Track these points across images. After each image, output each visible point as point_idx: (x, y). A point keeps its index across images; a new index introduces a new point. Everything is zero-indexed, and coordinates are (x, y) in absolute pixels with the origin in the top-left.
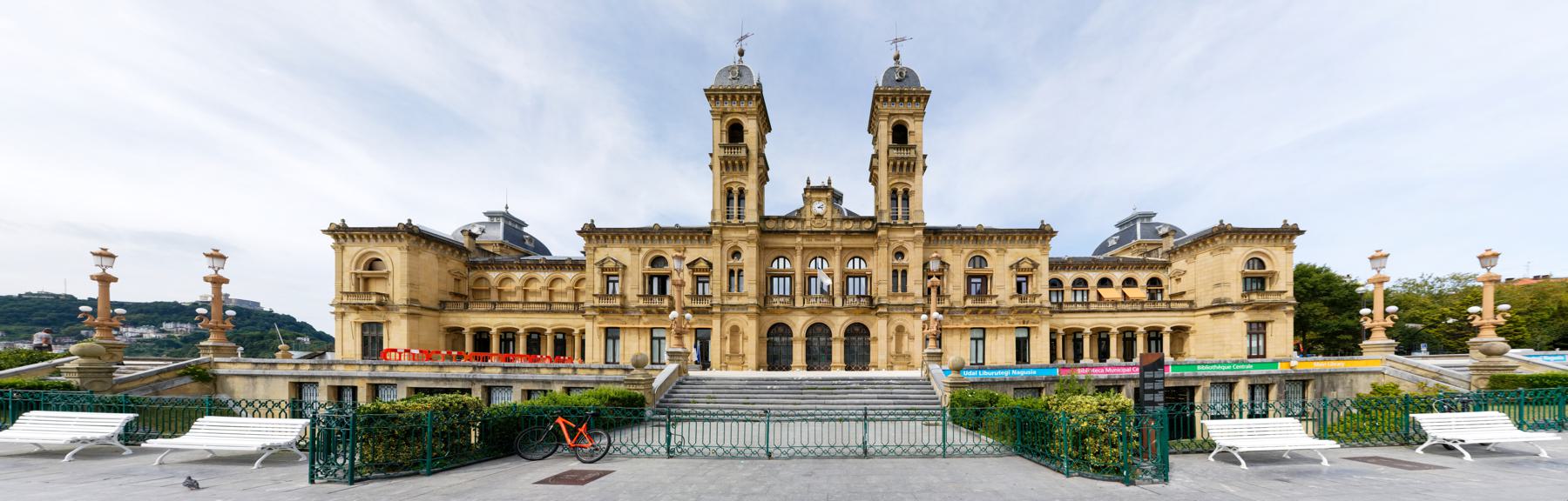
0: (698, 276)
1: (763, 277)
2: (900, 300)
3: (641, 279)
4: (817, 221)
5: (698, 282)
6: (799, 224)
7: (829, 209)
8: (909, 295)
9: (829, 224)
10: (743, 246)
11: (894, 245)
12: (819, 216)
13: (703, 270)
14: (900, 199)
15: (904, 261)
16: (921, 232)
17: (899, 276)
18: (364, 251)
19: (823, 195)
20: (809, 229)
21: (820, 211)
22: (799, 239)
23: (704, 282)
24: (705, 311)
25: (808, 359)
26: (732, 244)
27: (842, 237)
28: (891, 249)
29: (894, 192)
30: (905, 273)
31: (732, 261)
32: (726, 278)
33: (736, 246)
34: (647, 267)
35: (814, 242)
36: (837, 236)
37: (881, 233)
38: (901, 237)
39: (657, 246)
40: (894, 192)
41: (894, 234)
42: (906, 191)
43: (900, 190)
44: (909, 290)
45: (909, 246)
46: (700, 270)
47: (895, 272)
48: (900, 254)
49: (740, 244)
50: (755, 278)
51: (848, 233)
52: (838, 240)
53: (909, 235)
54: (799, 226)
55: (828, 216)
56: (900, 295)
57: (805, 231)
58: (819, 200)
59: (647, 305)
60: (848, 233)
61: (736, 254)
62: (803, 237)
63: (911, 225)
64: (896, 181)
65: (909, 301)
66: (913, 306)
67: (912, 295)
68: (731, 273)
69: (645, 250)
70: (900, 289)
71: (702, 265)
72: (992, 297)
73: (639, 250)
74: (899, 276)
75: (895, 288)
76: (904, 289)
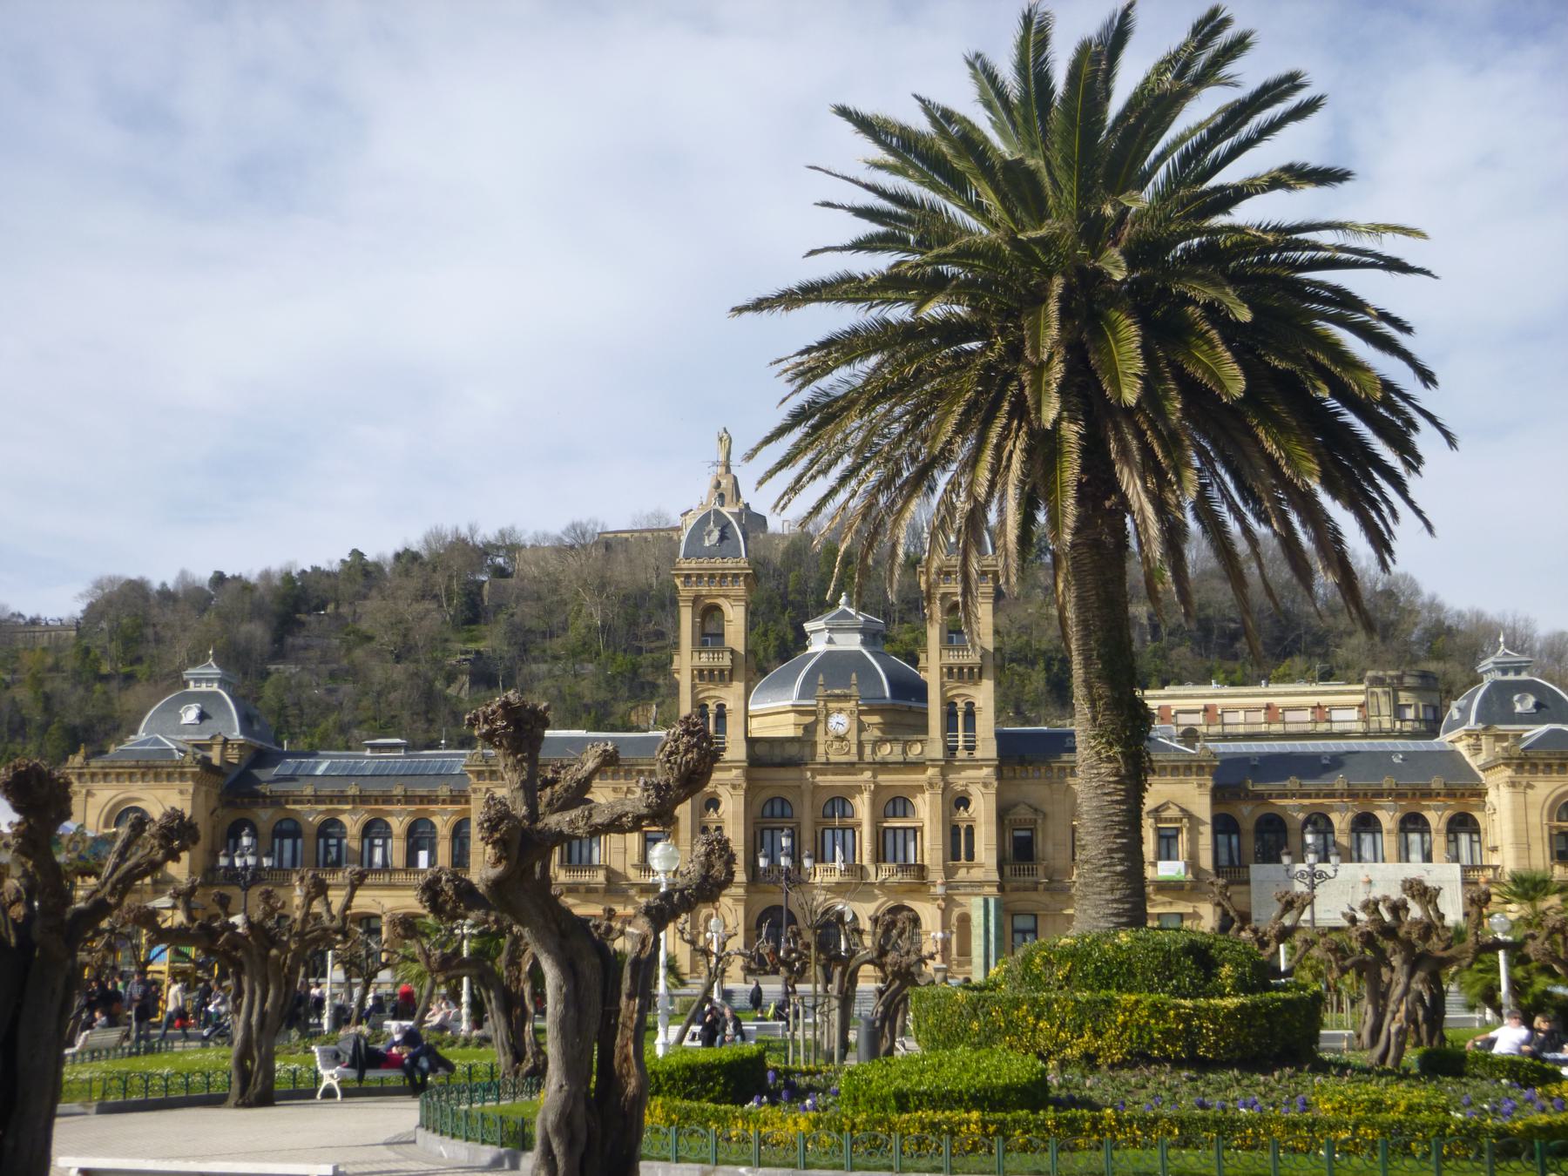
1: (751, 832)
4: (836, 745)
9: (854, 749)
18: (121, 797)
21: (841, 730)
30: (970, 831)
51: (884, 766)
58: (840, 711)
60: (884, 766)
67: (980, 866)
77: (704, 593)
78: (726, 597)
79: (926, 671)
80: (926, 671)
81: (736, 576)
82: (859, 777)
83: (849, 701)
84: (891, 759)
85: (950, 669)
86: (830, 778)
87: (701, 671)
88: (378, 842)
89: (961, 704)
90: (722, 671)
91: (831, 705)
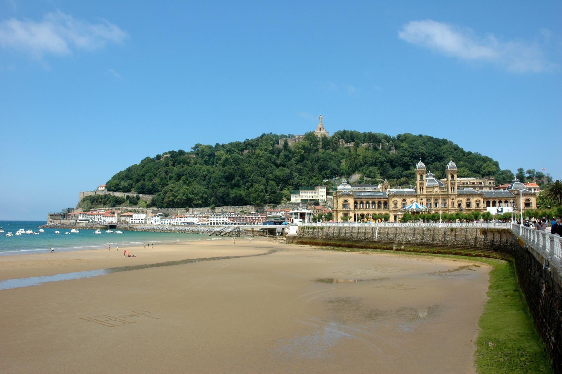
2: (453, 209)
10: (423, 198)
11: (451, 198)
12: (437, 192)
17: (453, 204)
19: (437, 187)
21: (437, 190)
22: (433, 196)
30: (454, 203)
39: (404, 197)
40: (452, 187)
47: (452, 203)
51: (442, 195)
52: (440, 196)
54: (433, 193)
65: (455, 209)
66: (455, 210)
72: (471, 207)
74: (453, 204)
76: (454, 206)
88: (367, 204)
89: (453, 188)
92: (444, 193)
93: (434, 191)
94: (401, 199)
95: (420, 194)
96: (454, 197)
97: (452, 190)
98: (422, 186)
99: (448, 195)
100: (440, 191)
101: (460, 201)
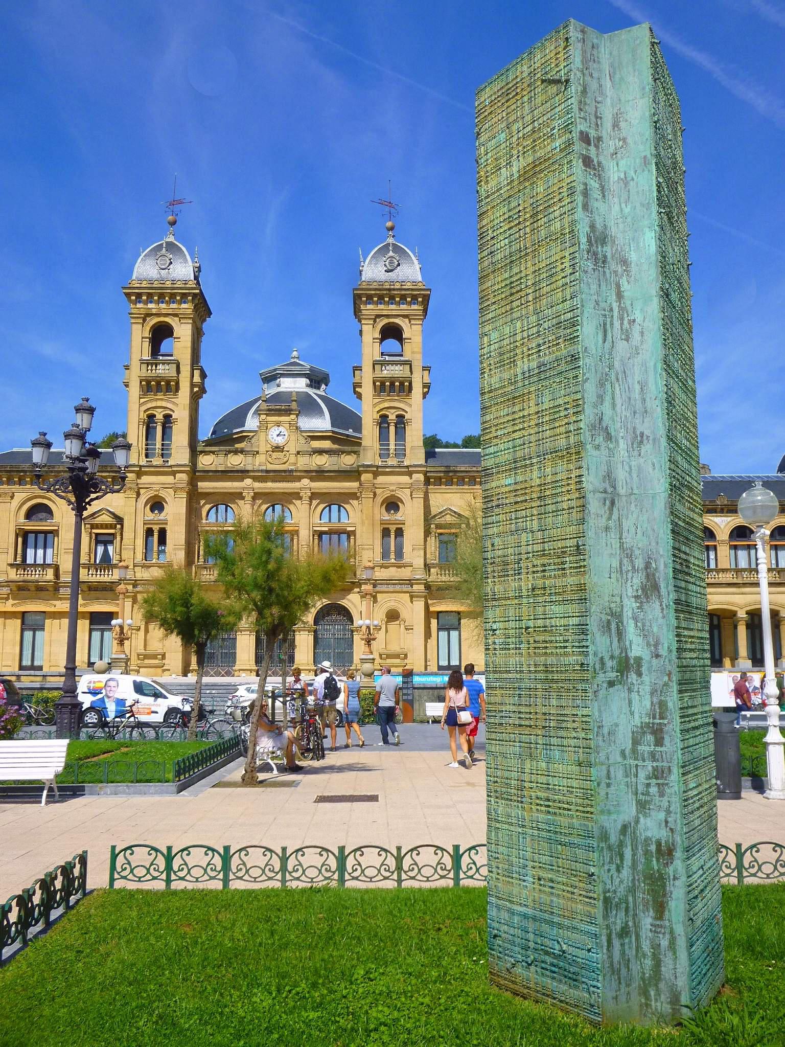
0: (97, 535)
2: (392, 573)
3: (13, 537)
4: (275, 455)
5: (98, 542)
6: (249, 459)
7: (293, 438)
8: (404, 566)
9: (292, 459)
10: (167, 495)
11: (382, 495)
12: (278, 449)
13: (107, 526)
14: (392, 429)
15: (399, 516)
16: (421, 477)
20: (264, 468)
21: (280, 441)
23: (106, 543)
24: (107, 590)
25: (258, 660)
26: (151, 493)
27: (312, 479)
28: (379, 500)
29: (384, 418)
30: (399, 533)
31: (150, 516)
32: (140, 542)
33: (156, 496)
34: (22, 519)
35: (270, 486)
36: (304, 477)
37: (364, 477)
38: (390, 483)
40: (384, 418)
41: (381, 479)
42: (400, 417)
43: (392, 417)
44: (407, 558)
45: (404, 495)
46: (102, 526)
48: (392, 505)
49: (162, 494)
50: (183, 542)
52: (305, 482)
53: (405, 479)
55: (292, 448)
56: (393, 565)
57: (258, 471)
58: (278, 424)
59: (22, 578)
61: (157, 505)
62: (255, 479)
63: (407, 467)
64: (386, 405)
65: (406, 573)
66: (410, 582)
68: (149, 532)
69: (20, 497)
70: (392, 556)
71: (105, 519)
73: (12, 497)
75: (385, 554)
77: (154, 311)
78: (176, 315)
79: (361, 387)
80: (361, 387)
81: (184, 296)
82: (297, 485)
83: (289, 415)
84: (327, 467)
85: (383, 384)
86: (270, 485)
87: (148, 382)
89: (392, 417)
90: (168, 383)
91: (270, 418)
92: (334, 459)
93: (262, 449)
94: (20, 497)
95: (143, 461)
96: (401, 487)
97: (383, 436)
98: (160, 404)
99: (353, 474)
100: (306, 448)
101: (448, 519)
